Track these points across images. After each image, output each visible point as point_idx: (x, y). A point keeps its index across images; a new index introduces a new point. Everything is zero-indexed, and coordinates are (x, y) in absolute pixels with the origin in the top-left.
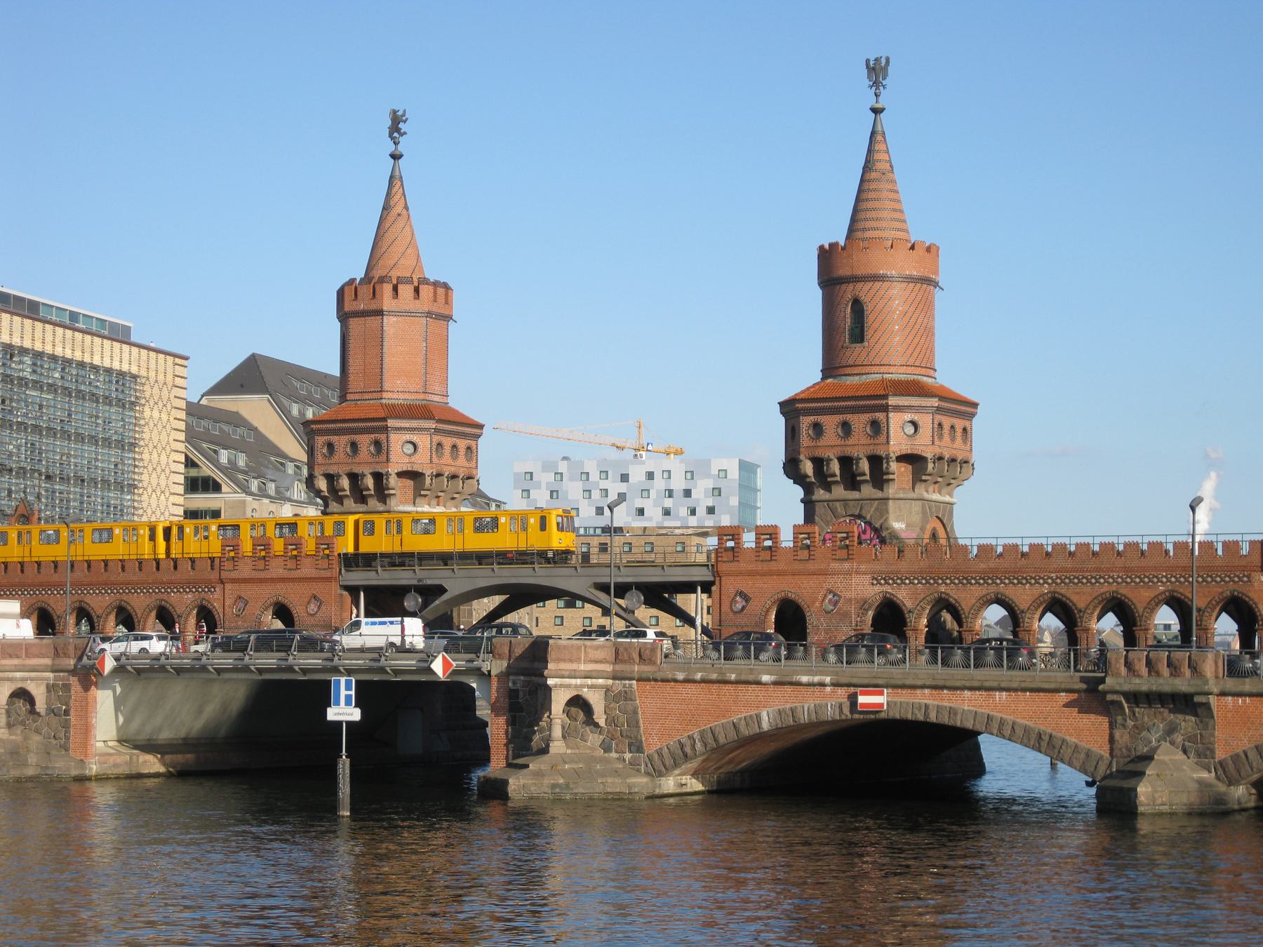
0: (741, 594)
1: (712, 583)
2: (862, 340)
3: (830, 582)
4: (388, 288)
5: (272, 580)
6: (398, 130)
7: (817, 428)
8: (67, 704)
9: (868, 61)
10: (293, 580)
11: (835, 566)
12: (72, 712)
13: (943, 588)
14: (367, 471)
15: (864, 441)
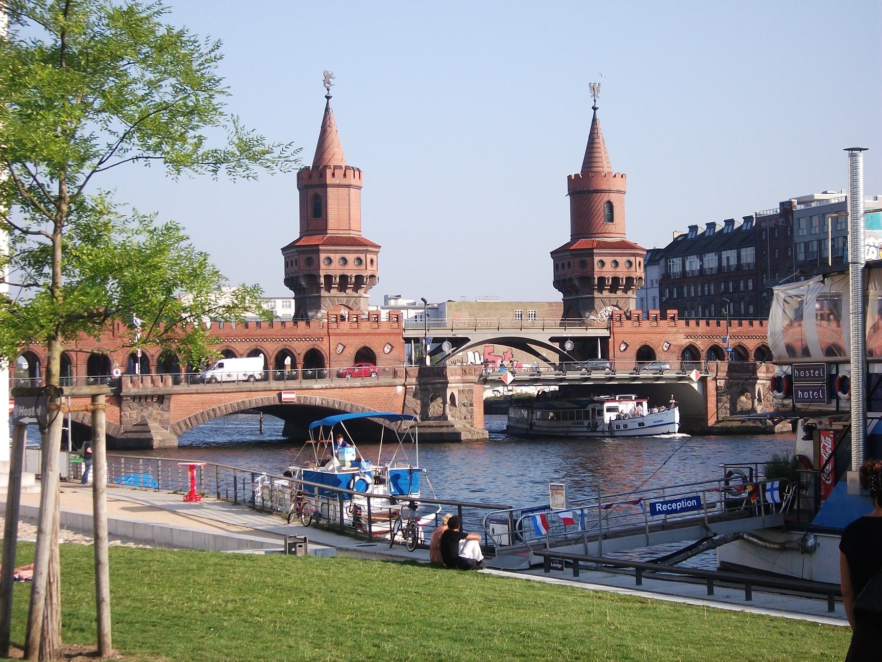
0: (625, 343)
1: (609, 337)
2: (612, 221)
3: (667, 337)
4: (329, 172)
5: (363, 334)
6: (329, 83)
7: (603, 263)
8: (471, 401)
9: (590, 83)
10: (376, 334)
11: (670, 329)
12: (474, 405)
13: (716, 340)
14: (354, 275)
15: (626, 270)
